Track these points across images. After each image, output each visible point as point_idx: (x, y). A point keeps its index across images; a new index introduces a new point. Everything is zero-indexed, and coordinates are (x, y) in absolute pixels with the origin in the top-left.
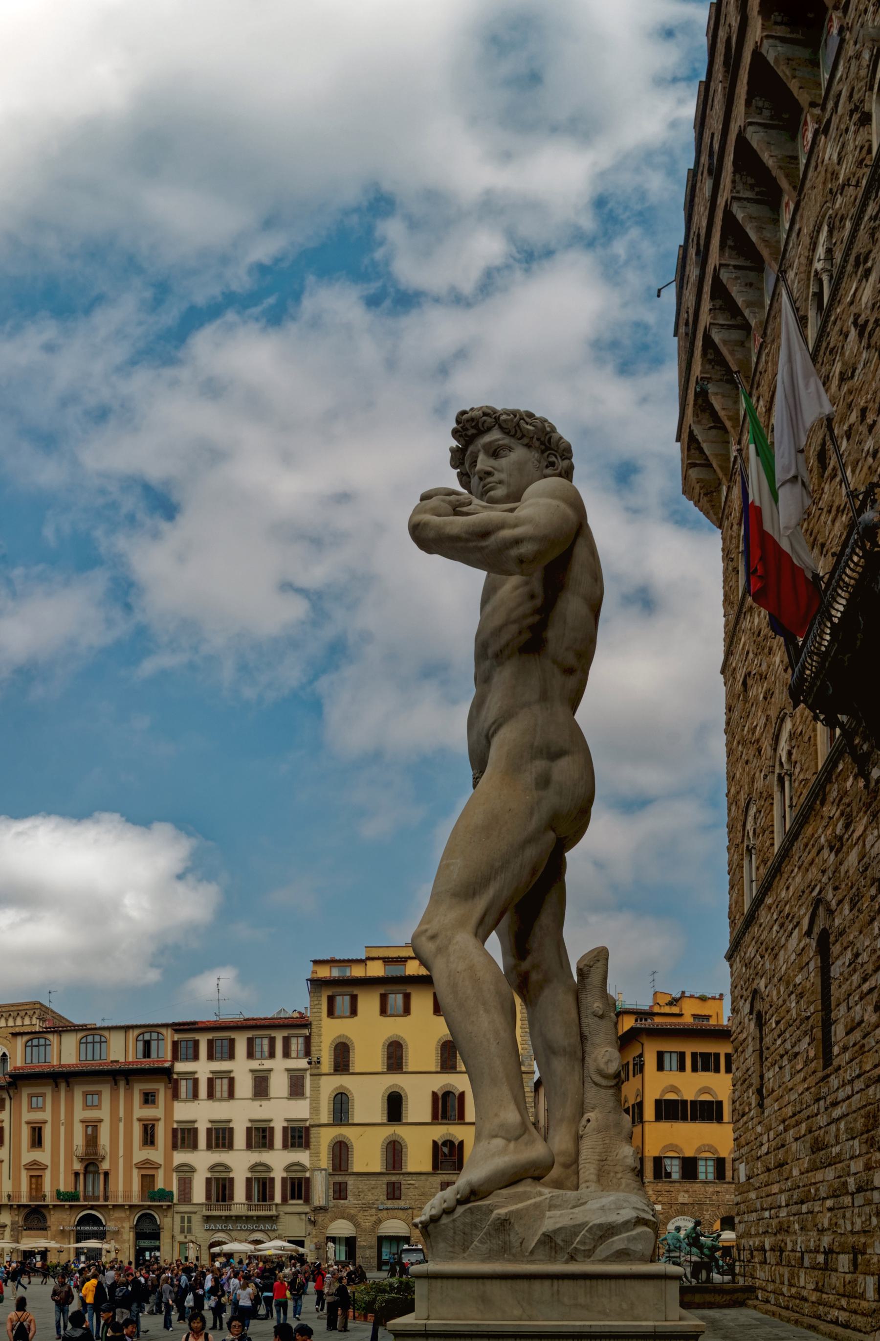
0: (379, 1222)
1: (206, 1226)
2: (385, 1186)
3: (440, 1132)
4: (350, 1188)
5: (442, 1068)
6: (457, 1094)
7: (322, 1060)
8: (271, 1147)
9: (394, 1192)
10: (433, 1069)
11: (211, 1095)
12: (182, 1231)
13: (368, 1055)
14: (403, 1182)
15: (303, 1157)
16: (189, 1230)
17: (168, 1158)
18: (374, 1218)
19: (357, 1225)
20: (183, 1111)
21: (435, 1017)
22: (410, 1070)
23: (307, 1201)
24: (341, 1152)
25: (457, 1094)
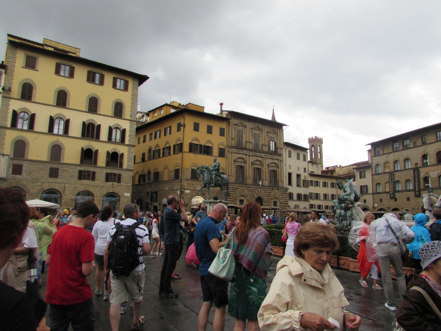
2: (48, 170)
3: (86, 144)
4: (24, 168)
5: (89, 110)
6: (96, 125)
7: (12, 89)
10: (84, 109)
14: (60, 168)
21: (87, 83)
22: (71, 107)
25: (96, 125)
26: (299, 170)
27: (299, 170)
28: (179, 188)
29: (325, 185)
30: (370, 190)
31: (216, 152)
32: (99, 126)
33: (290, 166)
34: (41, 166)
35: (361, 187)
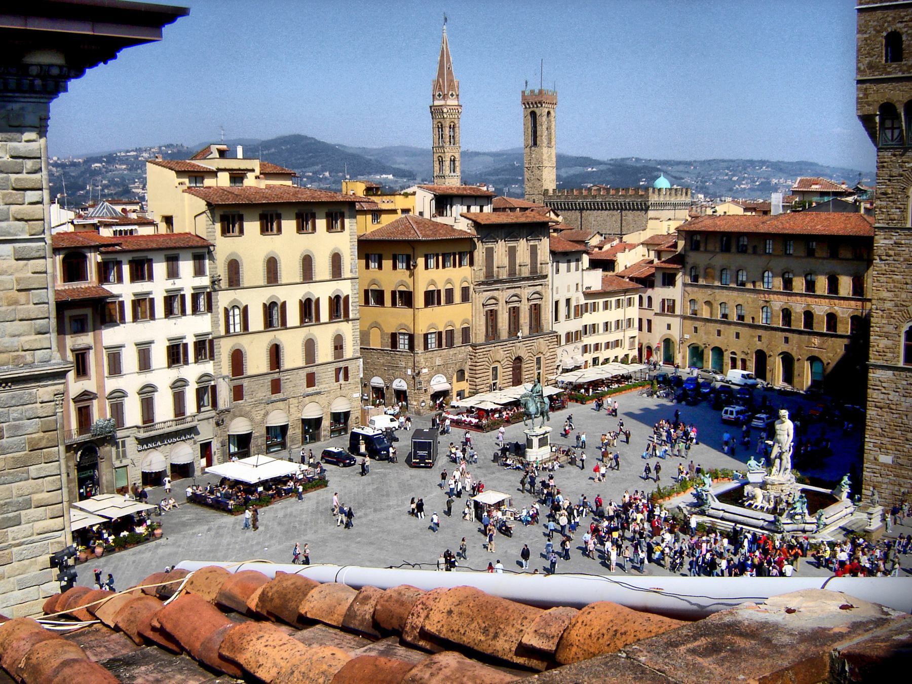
0: (266, 414)
1: (140, 447)
4: (245, 389)
5: (304, 279)
8: (186, 362)
9: (276, 387)
11: (135, 318)
12: (118, 457)
13: (253, 272)
15: (208, 367)
16: (124, 455)
17: (101, 386)
18: (263, 412)
19: (251, 420)
20: (110, 336)
22: (283, 282)
23: (214, 404)
24: (238, 358)
25: (314, 300)
26: (569, 290)
27: (569, 290)
28: (410, 364)
29: (606, 306)
30: (678, 311)
31: (457, 296)
32: (318, 300)
33: (557, 288)
34: (261, 380)
35: (663, 300)
